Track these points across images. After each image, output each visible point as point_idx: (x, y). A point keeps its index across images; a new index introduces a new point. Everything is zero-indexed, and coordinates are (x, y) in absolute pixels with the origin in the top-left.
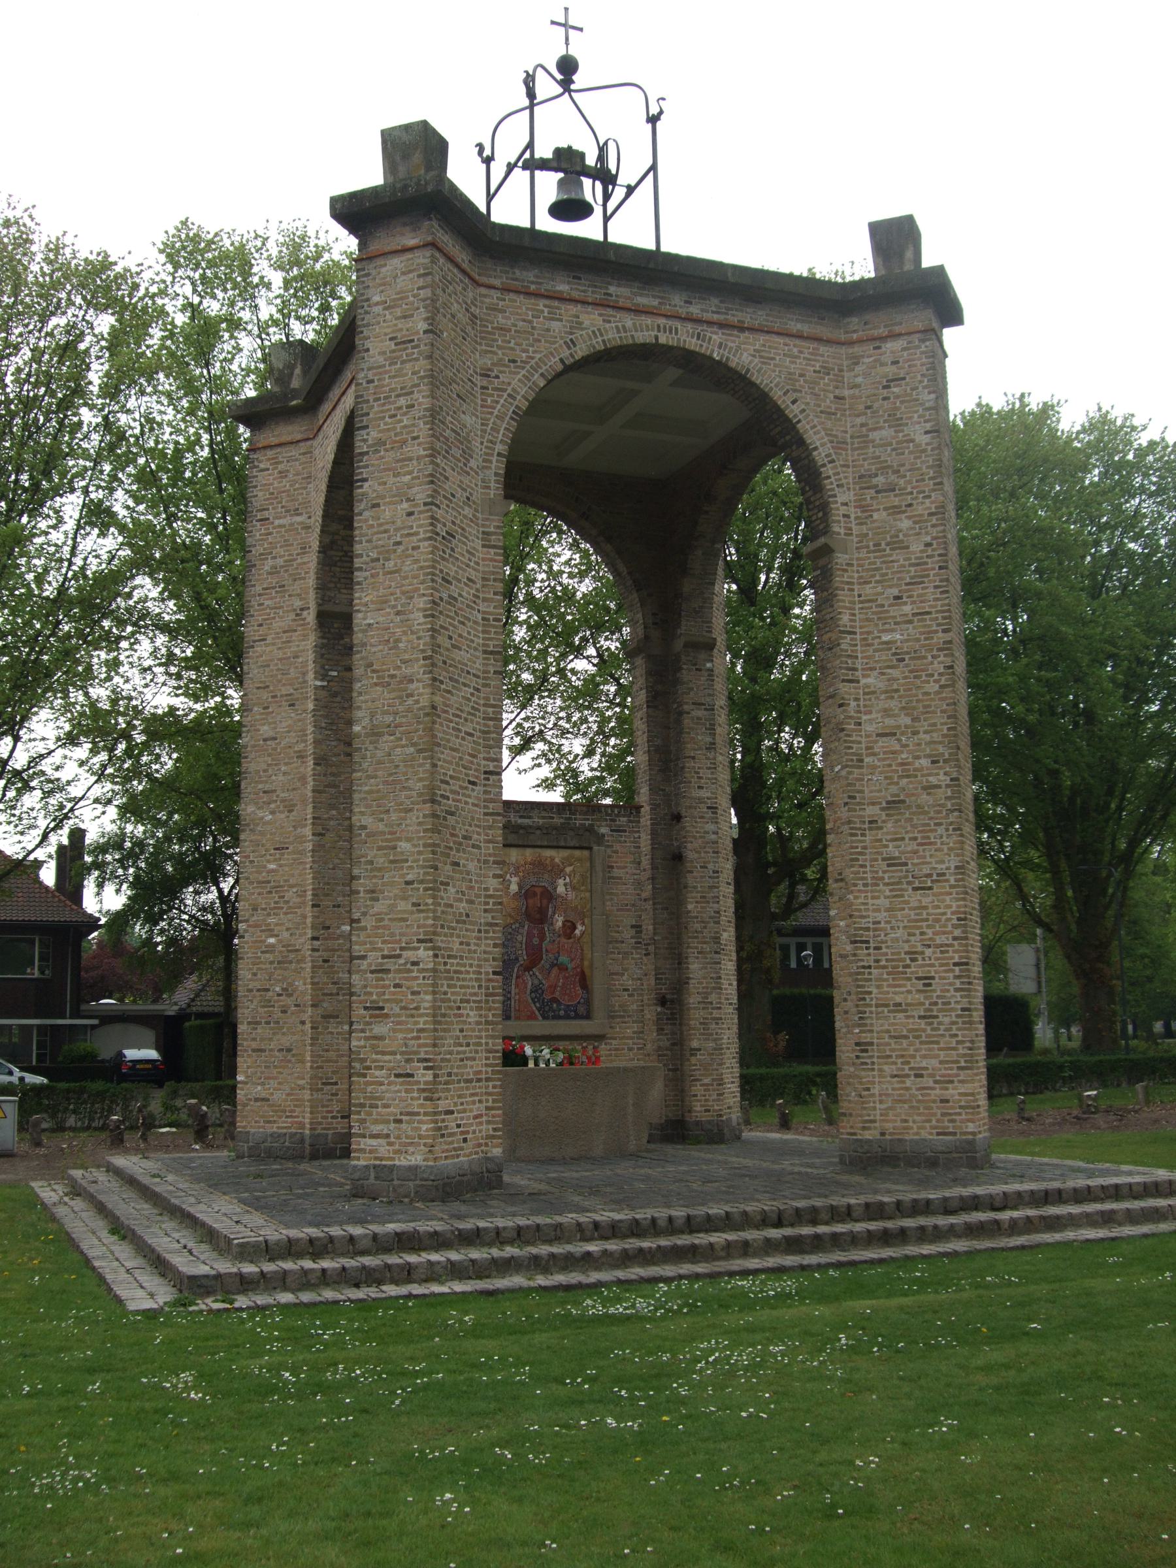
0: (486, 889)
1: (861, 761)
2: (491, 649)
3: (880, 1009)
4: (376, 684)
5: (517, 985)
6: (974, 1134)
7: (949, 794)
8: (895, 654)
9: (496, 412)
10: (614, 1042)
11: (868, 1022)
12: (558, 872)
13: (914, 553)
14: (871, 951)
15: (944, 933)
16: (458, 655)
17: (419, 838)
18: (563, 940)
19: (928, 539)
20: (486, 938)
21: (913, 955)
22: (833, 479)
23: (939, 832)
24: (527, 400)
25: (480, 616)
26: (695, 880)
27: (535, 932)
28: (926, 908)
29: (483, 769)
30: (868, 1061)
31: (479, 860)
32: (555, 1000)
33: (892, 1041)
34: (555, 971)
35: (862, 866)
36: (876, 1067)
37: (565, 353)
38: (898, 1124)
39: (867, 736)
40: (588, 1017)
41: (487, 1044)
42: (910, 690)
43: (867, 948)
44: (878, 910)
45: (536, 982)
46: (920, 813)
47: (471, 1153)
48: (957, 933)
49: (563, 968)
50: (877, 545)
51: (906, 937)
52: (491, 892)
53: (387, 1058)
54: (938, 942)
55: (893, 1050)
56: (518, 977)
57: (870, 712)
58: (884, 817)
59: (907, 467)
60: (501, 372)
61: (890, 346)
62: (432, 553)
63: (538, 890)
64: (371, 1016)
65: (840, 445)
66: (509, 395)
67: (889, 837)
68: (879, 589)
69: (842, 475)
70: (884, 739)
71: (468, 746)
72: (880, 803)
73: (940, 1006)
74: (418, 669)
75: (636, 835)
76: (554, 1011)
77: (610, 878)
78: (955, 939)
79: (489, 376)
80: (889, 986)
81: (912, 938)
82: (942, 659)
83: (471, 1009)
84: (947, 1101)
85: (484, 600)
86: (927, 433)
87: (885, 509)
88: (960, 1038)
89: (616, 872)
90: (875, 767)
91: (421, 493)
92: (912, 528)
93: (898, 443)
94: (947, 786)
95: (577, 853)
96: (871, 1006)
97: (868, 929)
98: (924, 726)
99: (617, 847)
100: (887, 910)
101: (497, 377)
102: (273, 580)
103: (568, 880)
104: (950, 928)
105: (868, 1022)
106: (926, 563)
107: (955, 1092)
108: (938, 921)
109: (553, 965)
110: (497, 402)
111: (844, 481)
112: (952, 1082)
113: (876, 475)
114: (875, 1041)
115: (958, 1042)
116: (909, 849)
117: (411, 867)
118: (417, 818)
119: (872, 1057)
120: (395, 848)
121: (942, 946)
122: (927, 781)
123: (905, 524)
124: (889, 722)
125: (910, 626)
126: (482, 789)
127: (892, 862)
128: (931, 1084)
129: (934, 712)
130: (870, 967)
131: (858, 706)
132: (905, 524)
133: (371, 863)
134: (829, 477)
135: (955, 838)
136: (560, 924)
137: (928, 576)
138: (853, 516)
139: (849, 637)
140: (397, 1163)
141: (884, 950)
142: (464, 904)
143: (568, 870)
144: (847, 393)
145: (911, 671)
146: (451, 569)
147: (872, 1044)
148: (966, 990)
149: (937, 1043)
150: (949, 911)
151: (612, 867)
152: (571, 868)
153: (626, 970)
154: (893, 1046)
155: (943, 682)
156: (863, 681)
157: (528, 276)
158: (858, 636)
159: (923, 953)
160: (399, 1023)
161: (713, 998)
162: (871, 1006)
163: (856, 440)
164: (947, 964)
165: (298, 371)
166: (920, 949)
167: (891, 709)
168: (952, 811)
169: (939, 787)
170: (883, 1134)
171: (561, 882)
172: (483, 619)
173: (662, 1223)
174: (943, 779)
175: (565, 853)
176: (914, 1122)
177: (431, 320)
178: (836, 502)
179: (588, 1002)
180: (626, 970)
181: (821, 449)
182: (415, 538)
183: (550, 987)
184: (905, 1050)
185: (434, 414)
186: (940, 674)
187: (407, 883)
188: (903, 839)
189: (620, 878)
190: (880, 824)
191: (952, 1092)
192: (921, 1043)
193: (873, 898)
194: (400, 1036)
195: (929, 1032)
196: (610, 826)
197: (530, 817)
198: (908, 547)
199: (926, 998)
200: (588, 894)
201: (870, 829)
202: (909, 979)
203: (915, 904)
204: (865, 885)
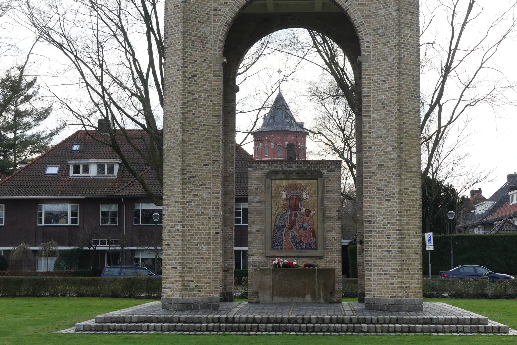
0: (213, 203)
1: (371, 148)
2: (216, 115)
3: (374, 247)
4: (169, 132)
5: (285, 236)
6: (401, 297)
7: (397, 162)
8: (383, 104)
9: (219, 24)
10: (328, 259)
11: (369, 252)
12: (304, 190)
13: (390, 62)
14: (372, 224)
15: (394, 218)
17: (179, 187)
18: (305, 217)
19: (394, 56)
20: (213, 220)
22: (362, 32)
23: (394, 177)
24: (231, 17)
25: (211, 103)
28: (389, 207)
29: (212, 159)
30: (369, 268)
31: (209, 193)
32: (301, 242)
33: (377, 260)
34: (302, 230)
35: (369, 191)
36: (372, 270)
38: (379, 293)
39: (373, 138)
40: (316, 249)
41: (213, 258)
42: (387, 119)
43: (370, 223)
44: (374, 208)
45: (293, 234)
46: (388, 170)
47: (203, 296)
48: (398, 218)
49: (305, 229)
50: (378, 59)
51: (382, 219)
52: (215, 204)
53: (171, 262)
54: (392, 221)
55: (378, 264)
56: (285, 232)
57: (374, 128)
58: (377, 171)
59: (389, 26)
60: (221, 8)
62: (183, 85)
63: (295, 197)
64: (167, 248)
65: (366, 17)
66: (225, 17)
67: (378, 179)
68: (378, 77)
69: (367, 30)
70: (378, 139)
71: (204, 151)
72: (376, 165)
73: (392, 247)
74: (179, 127)
75: (339, 173)
78: (397, 220)
79: (216, 10)
80: (377, 238)
81: (384, 219)
82: (397, 106)
83: (204, 245)
84: (394, 284)
85: (214, 96)
86: (396, 11)
87: (381, 43)
88: (398, 260)
89: (329, 189)
90: (375, 151)
91: (180, 62)
92: (390, 52)
93: (387, 15)
94: (397, 159)
95: (312, 181)
96: (371, 246)
97: (371, 216)
98: (390, 134)
99: (330, 178)
100: (377, 208)
101: (220, 10)
103: (307, 192)
104: (396, 216)
105: (369, 252)
106: (393, 66)
107: (396, 280)
108: (392, 213)
109: (300, 228)
110: (220, 20)
111: (368, 32)
112: (395, 277)
113: (379, 29)
114: (372, 260)
115: (397, 261)
116: (384, 184)
117: (177, 197)
119: (371, 266)
120: (173, 190)
121: (393, 223)
122: (391, 157)
123: (387, 50)
124: (380, 132)
125: (387, 92)
126: (212, 166)
127: (380, 189)
128: (389, 277)
129: (394, 128)
130: (371, 231)
131: (370, 126)
132: (387, 50)
133: (167, 195)
134: (361, 31)
135: (398, 180)
136: (304, 211)
137: (393, 72)
138: (371, 47)
139: (367, 97)
140: (173, 297)
141: (376, 224)
142: (201, 209)
143: (308, 188)
145: (387, 112)
147: (371, 261)
149: (391, 261)
150: (396, 209)
151: (328, 187)
152: (309, 187)
153: (334, 229)
154: (378, 262)
155: (397, 116)
156: (372, 115)
158: (371, 97)
159: (387, 225)
160: (174, 250)
162: (371, 246)
163: (373, 14)
164: (394, 230)
166: (386, 224)
167: (381, 127)
168: (398, 169)
169: (394, 159)
170: (374, 296)
171: (304, 193)
172: (213, 104)
173: (237, 319)
174: (394, 156)
175: (306, 181)
176: (383, 292)
178: (364, 42)
179: (316, 243)
180: (334, 229)
181: (357, 20)
182: (179, 79)
183: (299, 236)
184: (382, 264)
185: (184, 33)
186: (396, 113)
187: (176, 202)
188: (382, 180)
189: (332, 191)
190: (376, 174)
192: (386, 261)
193: (373, 203)
194: (174, 254)
195: (389, 257)
196: (327, 169)
197: (292, 167)
198: (388, 60)
199: (388, 243)
200: (316, 198)
201: (373, 176)
202: (383, 236)
203: (385, 206)
204: (370, 198)
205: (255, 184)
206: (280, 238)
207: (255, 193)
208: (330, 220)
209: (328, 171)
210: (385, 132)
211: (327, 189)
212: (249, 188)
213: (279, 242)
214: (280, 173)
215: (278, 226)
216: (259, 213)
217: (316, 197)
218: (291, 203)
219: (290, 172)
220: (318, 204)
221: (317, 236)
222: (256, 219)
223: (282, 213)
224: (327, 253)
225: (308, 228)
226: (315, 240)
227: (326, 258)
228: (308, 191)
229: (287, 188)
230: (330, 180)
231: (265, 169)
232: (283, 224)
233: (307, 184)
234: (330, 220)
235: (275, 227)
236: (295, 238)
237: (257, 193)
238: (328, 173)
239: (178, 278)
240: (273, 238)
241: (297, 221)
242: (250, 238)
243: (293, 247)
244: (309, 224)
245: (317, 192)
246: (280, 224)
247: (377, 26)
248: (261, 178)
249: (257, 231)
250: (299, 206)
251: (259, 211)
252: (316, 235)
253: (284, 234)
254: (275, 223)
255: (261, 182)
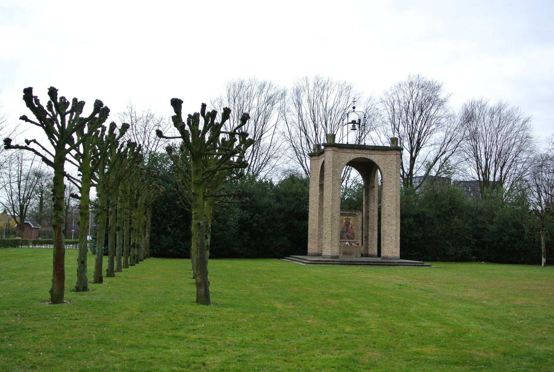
16: (336, 198)
21: (390, 234)
26: (370, 220)
37: (349, 160)
61: (391, 156)
65: (385, 168)
74: (331, 201)
89: (359, 220)
91: (331, 180)
102: (313, 179)
118: (330, 218)
123: (392, 180)
144: (386, 161)
146: (334, 189)
148: (396, 238)
157: (345, 150)
161: (372, 237)
165: (317, 149)
175: (351, 217)
177: (333, 160)
179: (354, 237)
191: (394, 250)
210: (390, 205)
219: (346, 214)
229: (345, 219)
239: (329, 248)
247: (388, 172)
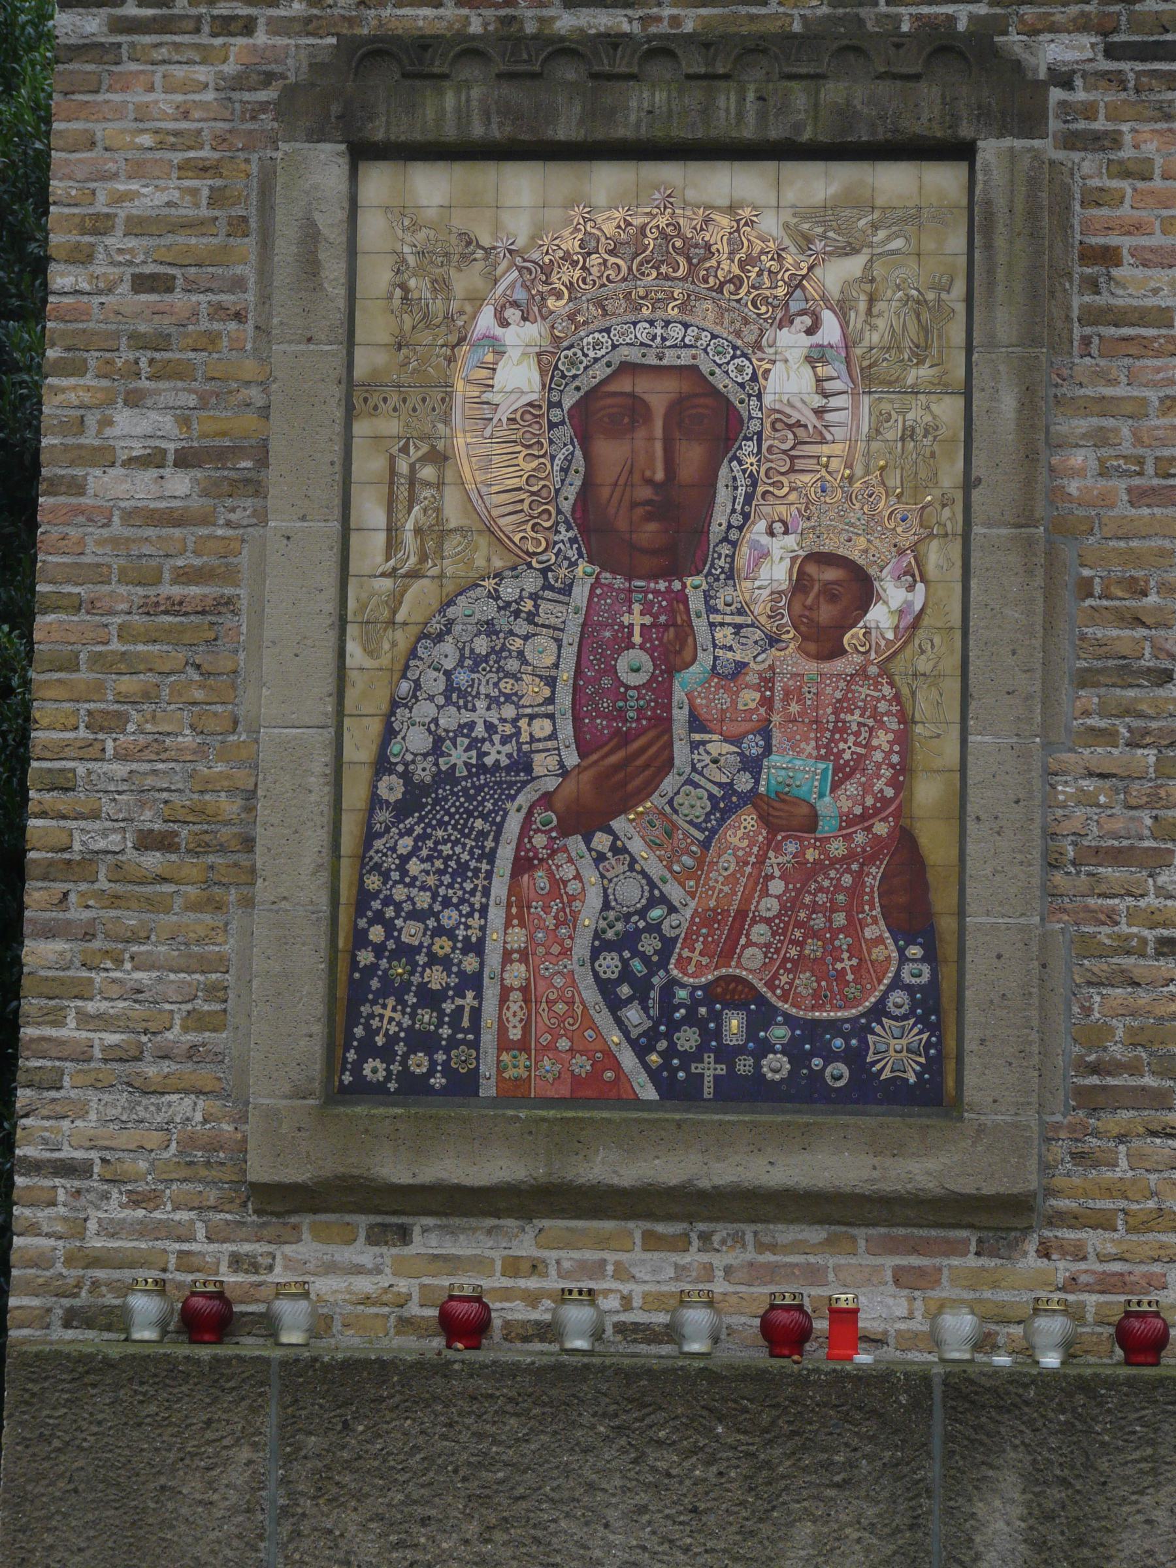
10: (1093, 1239)
27: (636, 618)
45: (630, 892)
56: (523, 864)
76: (726, 1055)
77: (1092, 316)
103: (831, 330)
151: (1109, 257)
152: (854, 266)
183: (708, 919)
200: (949, 410)
205: (137, 227)
206: (442, 946)
207: (140, 342)
208: (1128, 711)
209: (1111, 52)
211: (1093, 286)
212: (61, 278)
213: (430, 998)
214: (470, 71)
215: (423, 772)
216: (175, 607)
217: (942, 388)
218: (607, 474)
220: (969, 483)
221: (946, 924)
222: (128, 684)
223: (489, 610)
224: (1079, 1157)
225: (826, 806)
226: (918, 973)
227: (1074, 1220)
228: (842, 309)
230: (1140, 172)
231: (278, 27)
232: (496, 753)
233: (823, 214)
234: (1128, 711)
235: (392, 789)
236: (650, 945)
237: (160, 342)
238: (1117, 80)
240: (360, 939)
241: (680, 716)
242: (49, 933)
243: (628, 1060)
244: (848, 749)
245: (956, 333)
246: (458, 756)
248: (220, 140)
249: (147, 841)
250: (720, 518)
251: (184, 576)
252: (942, 900)
253: (500, 888)
254: (389, 733)
255: (217, 198)
